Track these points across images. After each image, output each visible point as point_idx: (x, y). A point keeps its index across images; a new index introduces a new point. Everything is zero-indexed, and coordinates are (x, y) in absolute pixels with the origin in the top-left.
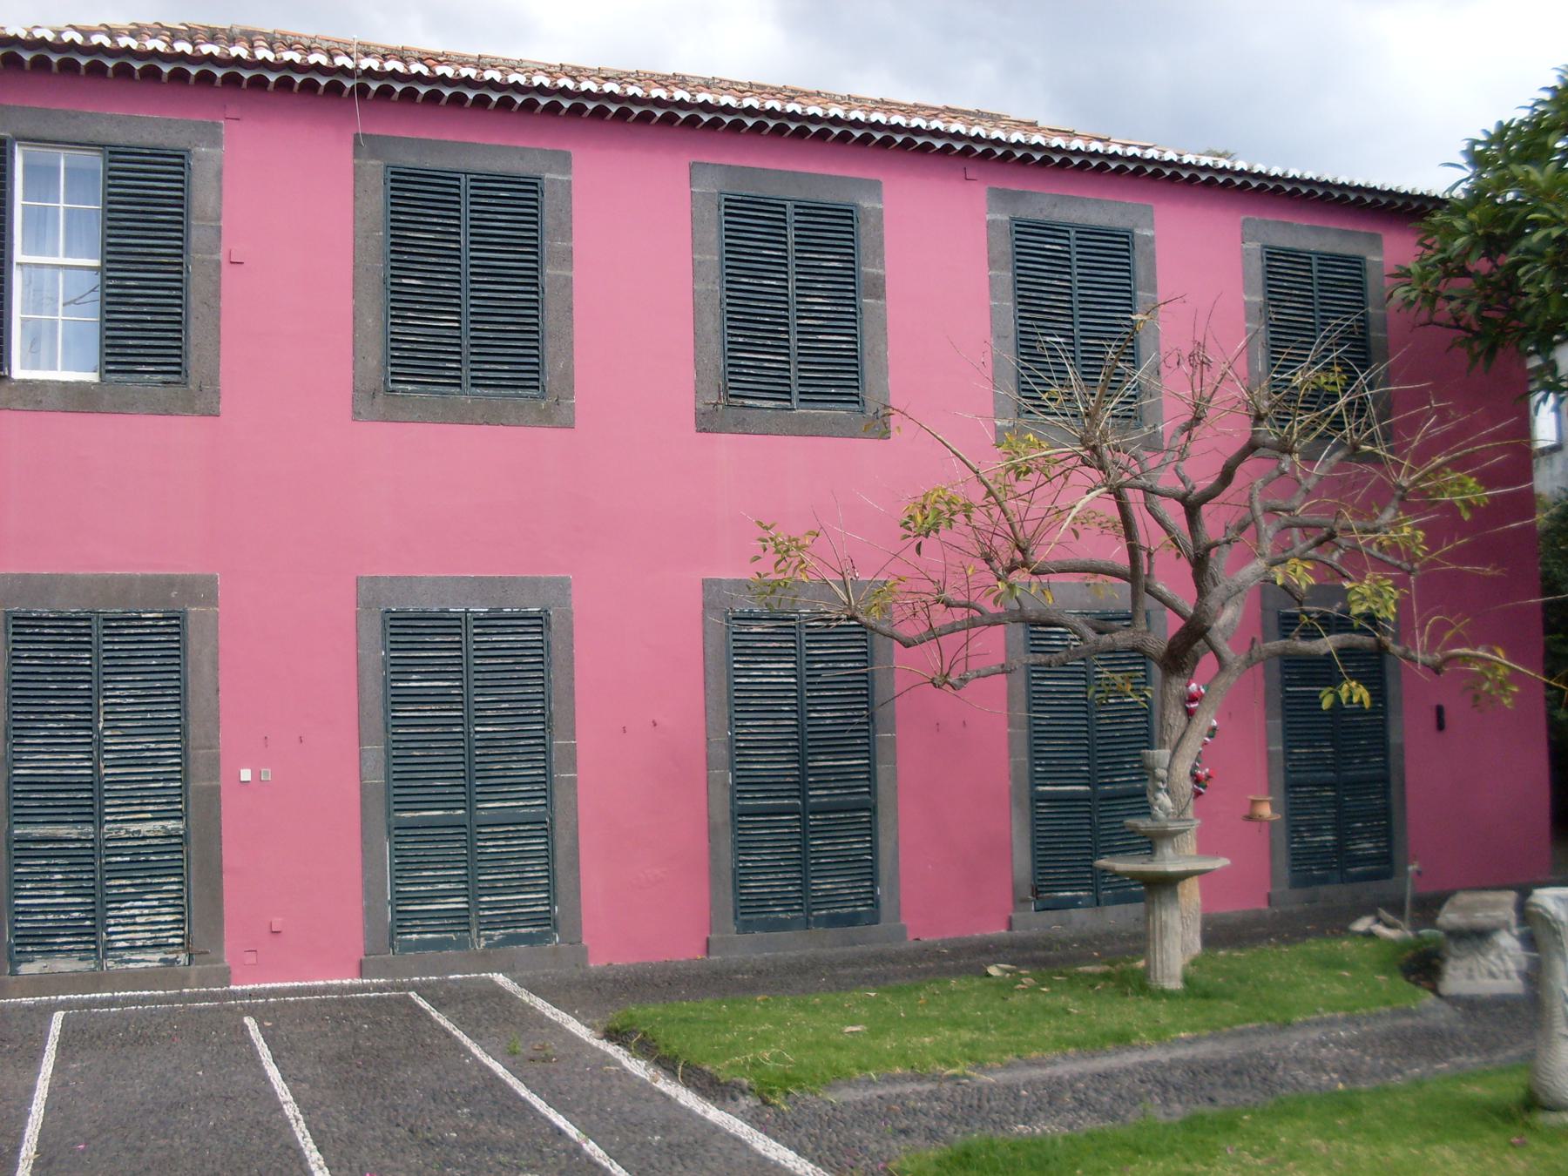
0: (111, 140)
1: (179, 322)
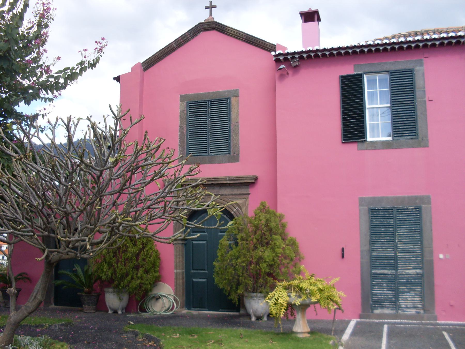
0: (391, 69)
1: (414, 120)
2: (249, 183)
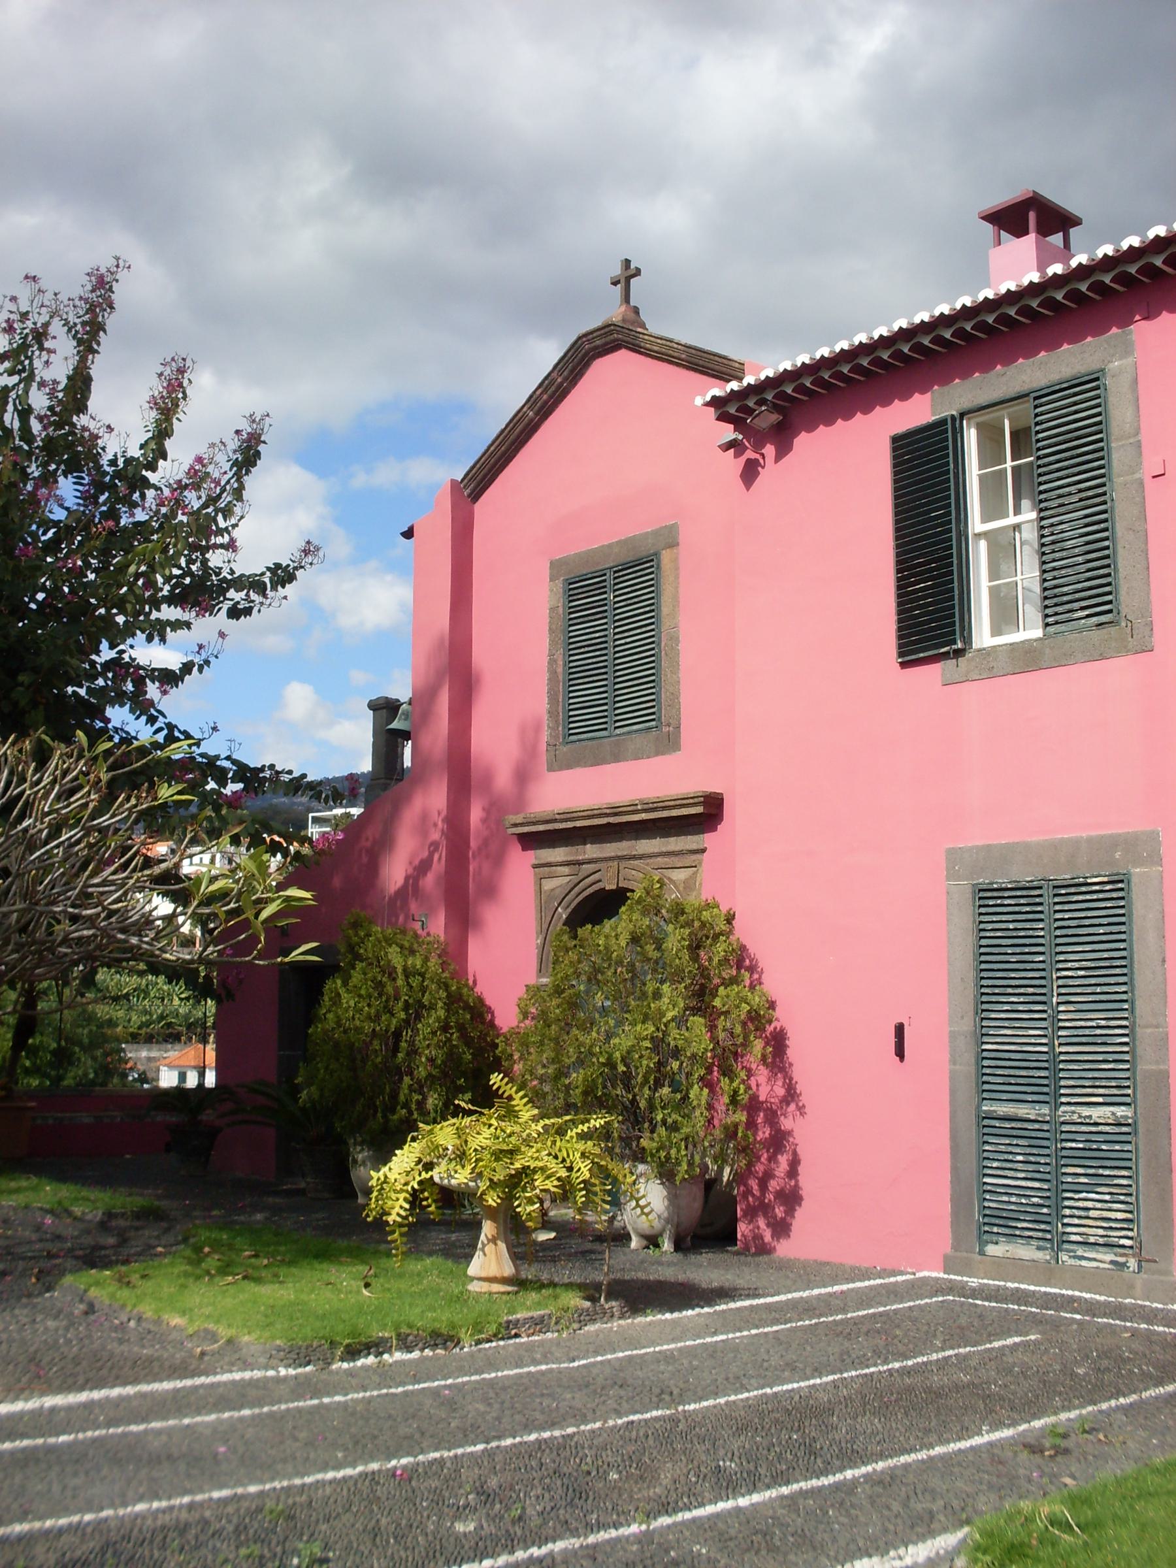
2: (708, 813)
